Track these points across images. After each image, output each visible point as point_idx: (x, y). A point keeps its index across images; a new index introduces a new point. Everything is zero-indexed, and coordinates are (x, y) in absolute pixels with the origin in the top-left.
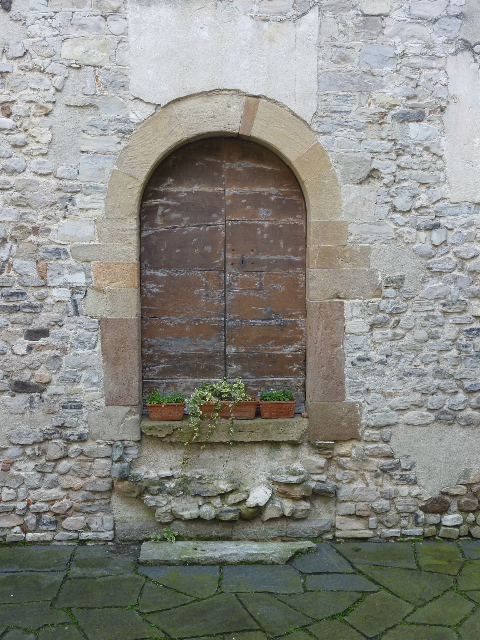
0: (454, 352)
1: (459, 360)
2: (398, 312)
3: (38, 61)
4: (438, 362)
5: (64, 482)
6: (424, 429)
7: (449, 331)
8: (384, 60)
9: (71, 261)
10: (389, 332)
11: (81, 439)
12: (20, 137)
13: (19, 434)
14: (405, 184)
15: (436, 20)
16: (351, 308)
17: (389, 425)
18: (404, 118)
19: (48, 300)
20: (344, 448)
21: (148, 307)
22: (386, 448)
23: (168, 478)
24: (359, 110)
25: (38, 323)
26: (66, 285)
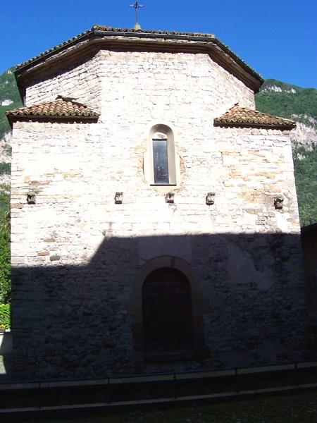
0: (236, 328)
18: (216, 261)
26: (121, 314)
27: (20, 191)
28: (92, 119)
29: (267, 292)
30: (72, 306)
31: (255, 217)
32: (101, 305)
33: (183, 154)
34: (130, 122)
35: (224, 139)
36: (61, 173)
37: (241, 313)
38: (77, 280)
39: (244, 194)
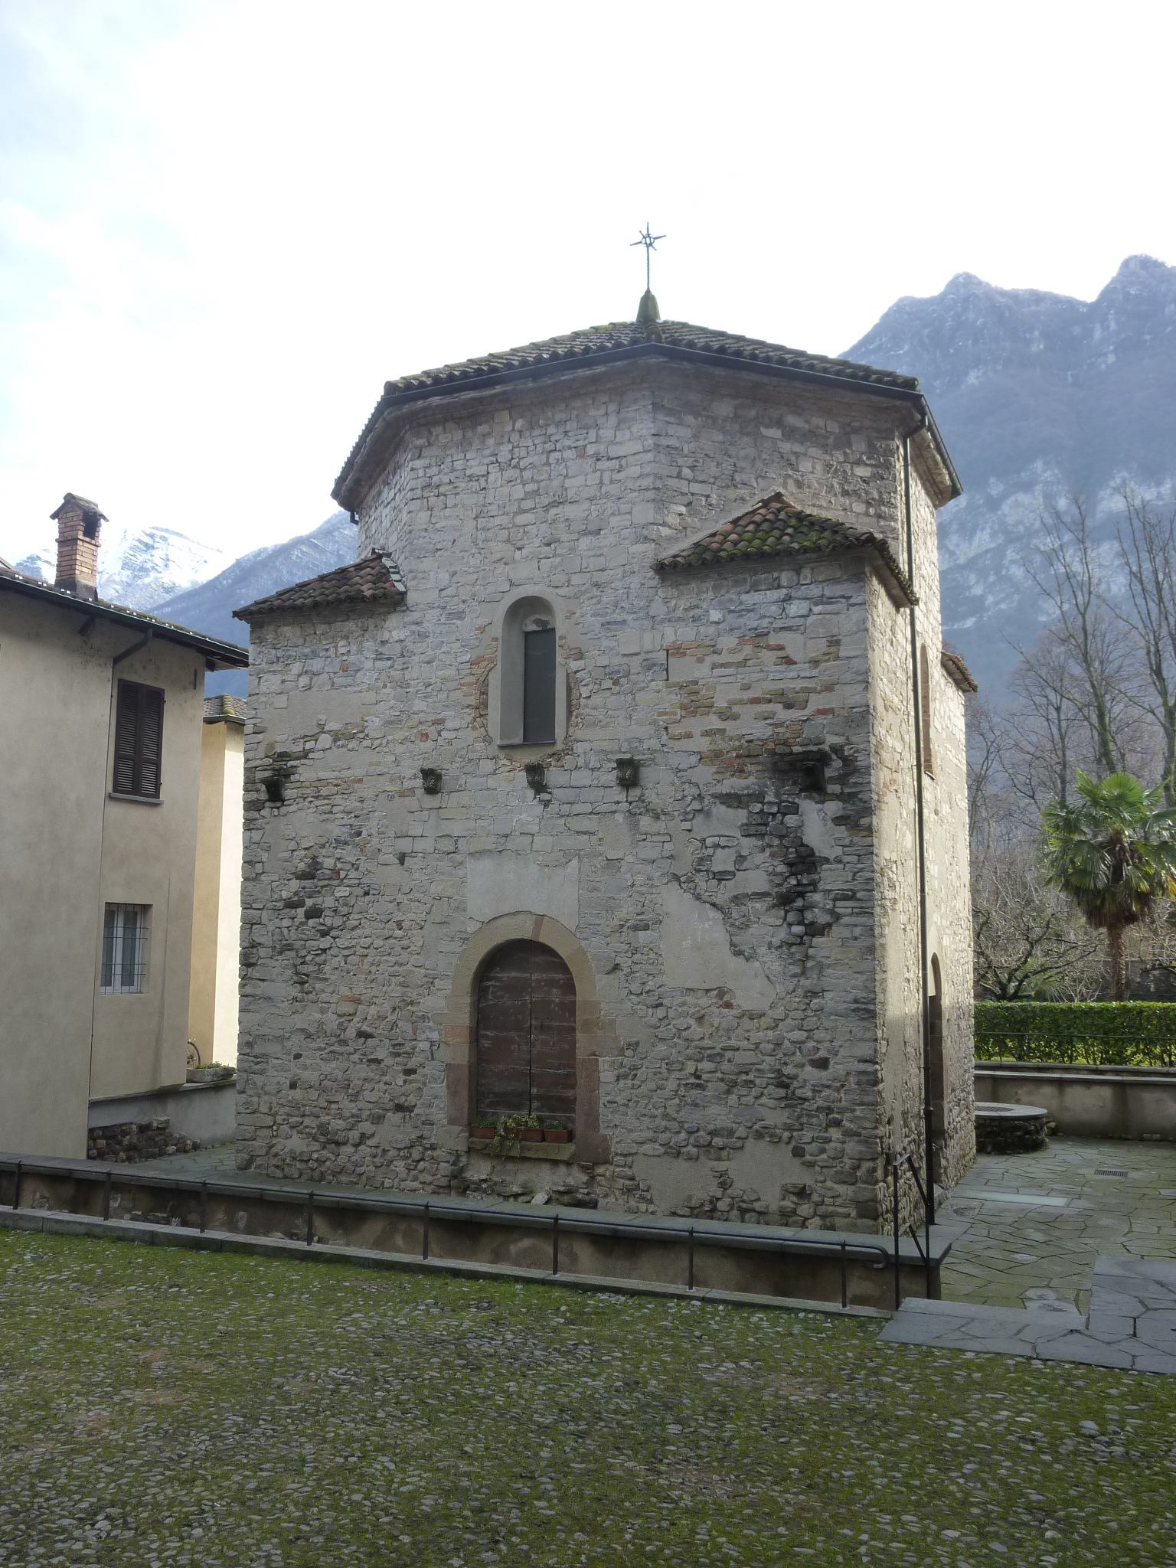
0: (677, 1101)
5: (421, 1178)
7: (671, 1085)
11: (433, 1148)
12: (405, 943)
16: (604, 1063)
18: (636, 928)
20: (600, 1170)
22: (629, 1172)
23: (485, 1181)
25: (411, 1065)
26: (427, 1039)
30: (340, 1016)
31: (741, 816)
32: (392, 1018)
33: (574, 665)
35: (679, 613)
39: (717, 755)
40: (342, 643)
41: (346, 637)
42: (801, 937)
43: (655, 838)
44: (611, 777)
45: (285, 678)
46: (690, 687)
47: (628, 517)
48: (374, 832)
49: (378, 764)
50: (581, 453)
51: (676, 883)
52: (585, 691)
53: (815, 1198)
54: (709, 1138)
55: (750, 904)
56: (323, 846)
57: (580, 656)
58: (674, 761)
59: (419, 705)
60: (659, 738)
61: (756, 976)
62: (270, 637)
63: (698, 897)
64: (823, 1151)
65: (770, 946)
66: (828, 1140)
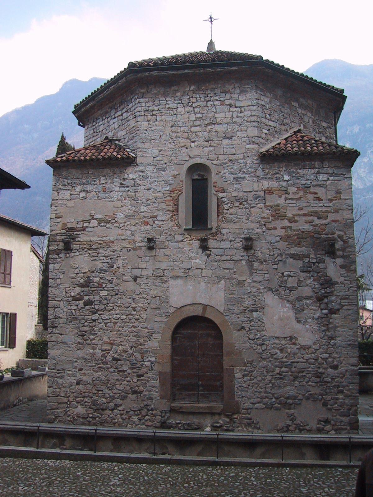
0: (271, 385)
1: (272, 388)
2: (252, 371)
3: (144, 295)
4: (266, 388)
5: (146, 424)
6: (262, 411)
7: (269, 378)
8: (244, 294)
9: (151, 354)
10: (249, 378)
11: (152, 410)
13: (134, 407)
14: (253, 331)
15: (260, 282)
16: (237, 369)
17: (250, 409)
18: (252, 311)
19: (144, 366)
20: (235, 416)
21: (174, 368)
22: (249, 416)
23: (179, 423)
24: (237, 309)
25: (140, 373)
26: (149, 361)
27: (58, 238)
28: (130, 162)
29: (309, 347)
30: (103, 351)
31: (300, 263)
32: (130, 351)
33: (221, 195)
34: (166, 163)
35: (269, 176)
36: (96, 219)
37: (277, 369)
38: (108, 324)
40: (102, 178)
41: (104, 176)
42: (327, 315)
43: (260, 272)
44: (239, 245)
45: (73, 193)
46: (276, 208)
47: (246, 132)
48: (121, 266)
49: (122, 235)
50: (222, 103)
51: (271, 292)
52: (226, 207)
53: (332, 422)
54: (285, 400)
55: (304, 301)
56: (93, 272)
57: (223, 191)
58: (269, 238)
59: (143, 209)
60: (262, 229)
61: (307, 331)
62: (64, 174)
63: (281, 298)
64: (336, 403)
65: (313, 318)
66: (338, 399)
